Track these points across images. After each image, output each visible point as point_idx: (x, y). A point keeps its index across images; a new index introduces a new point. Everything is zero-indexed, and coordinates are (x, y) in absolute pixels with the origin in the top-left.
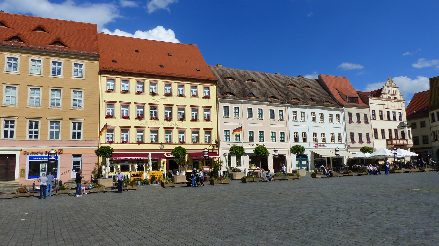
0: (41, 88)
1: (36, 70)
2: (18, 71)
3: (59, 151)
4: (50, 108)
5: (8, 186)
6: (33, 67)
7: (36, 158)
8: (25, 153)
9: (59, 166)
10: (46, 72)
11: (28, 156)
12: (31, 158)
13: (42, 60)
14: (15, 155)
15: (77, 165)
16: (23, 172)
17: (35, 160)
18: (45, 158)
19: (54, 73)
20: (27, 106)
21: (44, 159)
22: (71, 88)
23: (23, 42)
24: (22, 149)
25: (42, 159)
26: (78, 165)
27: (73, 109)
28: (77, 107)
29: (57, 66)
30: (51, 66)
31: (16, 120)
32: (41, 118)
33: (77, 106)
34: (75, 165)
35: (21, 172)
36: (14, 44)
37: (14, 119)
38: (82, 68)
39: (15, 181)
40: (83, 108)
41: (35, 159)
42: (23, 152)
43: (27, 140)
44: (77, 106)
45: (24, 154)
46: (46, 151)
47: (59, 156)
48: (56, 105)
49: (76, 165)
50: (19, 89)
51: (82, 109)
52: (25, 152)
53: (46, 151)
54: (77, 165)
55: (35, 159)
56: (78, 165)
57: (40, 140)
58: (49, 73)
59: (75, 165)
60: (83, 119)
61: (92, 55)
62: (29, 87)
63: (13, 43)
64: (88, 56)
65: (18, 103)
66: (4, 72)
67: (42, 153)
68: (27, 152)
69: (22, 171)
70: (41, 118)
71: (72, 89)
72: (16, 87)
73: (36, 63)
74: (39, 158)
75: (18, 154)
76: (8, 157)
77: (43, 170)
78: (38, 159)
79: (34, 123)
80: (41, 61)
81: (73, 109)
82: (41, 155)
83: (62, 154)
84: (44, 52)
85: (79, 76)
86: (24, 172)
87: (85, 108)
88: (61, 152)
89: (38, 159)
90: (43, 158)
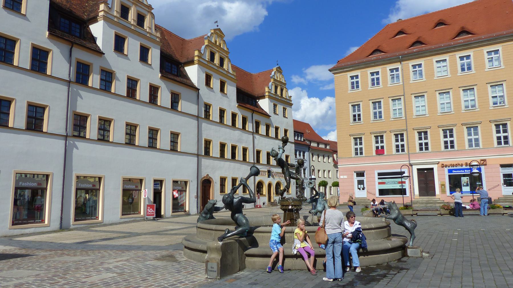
0: (451, 91)
1: (442, 71)
2: (424, 77)
3: (482, 162)
4: (464, 111)
5: (430, 202)
6: (439, 69)
7: (455, 172)
8: (443, 166)
9: (485, 180)
10: (454, 71)
11: (446, 170)
12: (450, 171)
13: (447, 58)
14: (432, 169)
15: (508, 179)
16: (443, 187)
17: (455, 173)
18: (466, 171)
19: (463, 69)
20: (438, 114)
21: (465, 172)
22: (487, 83)
23: (424, 44)
24: (439, 162)
25: (463, 172)
26: (509, 178)
27: (493, 108)
28: (499, 105)
29: (465, 61)
30: (459, 62)
31: (428, 131)
32: (455, 125)
33: (498, 103)
34: (505, 179)
35: (442, 187)
36: (416, 50)
37: (427, 130)
38: (498, 55)
39: (437, 197)
40: (507, 105)
41: (455, 173)
42: (440, 165)
43: (443, 152)
44: (498, 103)
45: (442, 167)
46: (466, 162)
47: (483, 168)
48: (471, 108)
49: (506, 178)
50: (427, 97)
51: (505, 107)
52: (443, 164)
53: (466, 163)
54: (508, 179)
55: (455, 173)
56: (509, 178)
57: (457, 150)
58: (457, 71)
59: (505, 179)
60: (510, 119)
61: (510, 35)
62: (437, 93)
63: (415, 49)
64: (504, 37)
65: (429, 112)
66: (411, 82)
67: (462, 165)
68: (445, 164)
69: (443, 186)
70: (455, 125)
71: (488, 84)
72: (424, 95)
73: (442, 64)
74: (459, 171)
75: (435, 167)
76: (426, 171)
77: (465, 184)
78: (458, 173)
79: (448, 132)
80: (446, 60)
81: (493, 108)
82: (461, 167)
83: (486, 165)
84: (448, 48)
85: (496, 66)
86: (445, 187)
87: (509, 104)
88: (485, 163)
89: (458, 173)
90: (463, 171)
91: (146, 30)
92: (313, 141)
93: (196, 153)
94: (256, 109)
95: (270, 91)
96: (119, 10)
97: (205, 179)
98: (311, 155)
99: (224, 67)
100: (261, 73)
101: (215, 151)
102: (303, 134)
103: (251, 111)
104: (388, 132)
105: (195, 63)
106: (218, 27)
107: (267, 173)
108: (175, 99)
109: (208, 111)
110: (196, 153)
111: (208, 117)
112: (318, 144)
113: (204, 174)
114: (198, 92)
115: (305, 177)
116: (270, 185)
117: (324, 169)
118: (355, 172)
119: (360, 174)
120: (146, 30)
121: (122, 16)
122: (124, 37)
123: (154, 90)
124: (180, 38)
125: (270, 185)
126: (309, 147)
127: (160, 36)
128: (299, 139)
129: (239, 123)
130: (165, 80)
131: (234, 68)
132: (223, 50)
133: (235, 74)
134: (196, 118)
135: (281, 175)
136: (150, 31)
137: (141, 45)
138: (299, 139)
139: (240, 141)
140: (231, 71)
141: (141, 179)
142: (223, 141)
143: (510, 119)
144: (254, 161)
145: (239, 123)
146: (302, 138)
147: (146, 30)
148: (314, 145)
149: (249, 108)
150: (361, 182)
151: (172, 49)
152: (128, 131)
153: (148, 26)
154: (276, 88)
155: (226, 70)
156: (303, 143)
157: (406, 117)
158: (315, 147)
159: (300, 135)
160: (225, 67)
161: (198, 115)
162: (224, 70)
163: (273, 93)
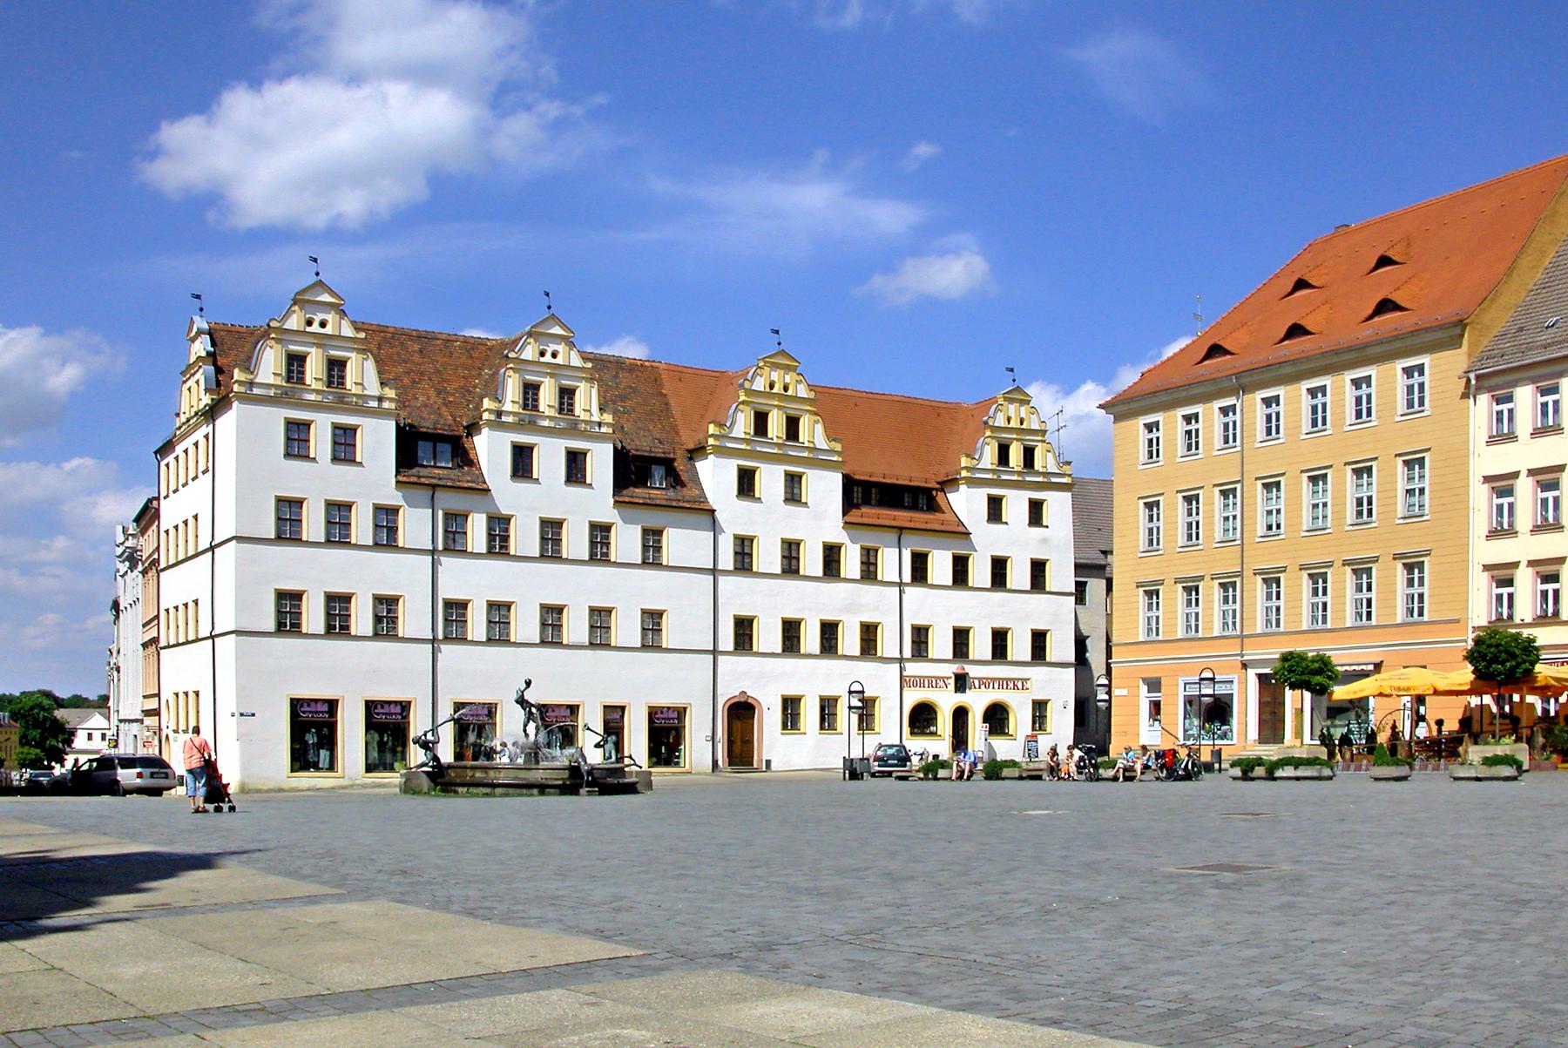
51: (1425, 518)
60: (1427, 553)
93: (712, 648)
96: (519, 397)
97: (738, 702)
101: (768, 636)
103: (896, 530)
104: (1207, 578)
106: (781, 347)
108: (652, 540)
109: (747, 554)
111: (746, 566)
113: (728, 692)
118: (1144, 680)
119: (1154, 685)
123: (600, 534)
124: (713, 371)
127: (611, 421)
129: (851, 563)
139: (850, 608)
140: (821, 442)
143: (1427, 553)
145: (851, 563)
150: (1156, 708)
152: (739, 550)
157: (1242, 540)
160: (804, 435)
163: (990, 467)
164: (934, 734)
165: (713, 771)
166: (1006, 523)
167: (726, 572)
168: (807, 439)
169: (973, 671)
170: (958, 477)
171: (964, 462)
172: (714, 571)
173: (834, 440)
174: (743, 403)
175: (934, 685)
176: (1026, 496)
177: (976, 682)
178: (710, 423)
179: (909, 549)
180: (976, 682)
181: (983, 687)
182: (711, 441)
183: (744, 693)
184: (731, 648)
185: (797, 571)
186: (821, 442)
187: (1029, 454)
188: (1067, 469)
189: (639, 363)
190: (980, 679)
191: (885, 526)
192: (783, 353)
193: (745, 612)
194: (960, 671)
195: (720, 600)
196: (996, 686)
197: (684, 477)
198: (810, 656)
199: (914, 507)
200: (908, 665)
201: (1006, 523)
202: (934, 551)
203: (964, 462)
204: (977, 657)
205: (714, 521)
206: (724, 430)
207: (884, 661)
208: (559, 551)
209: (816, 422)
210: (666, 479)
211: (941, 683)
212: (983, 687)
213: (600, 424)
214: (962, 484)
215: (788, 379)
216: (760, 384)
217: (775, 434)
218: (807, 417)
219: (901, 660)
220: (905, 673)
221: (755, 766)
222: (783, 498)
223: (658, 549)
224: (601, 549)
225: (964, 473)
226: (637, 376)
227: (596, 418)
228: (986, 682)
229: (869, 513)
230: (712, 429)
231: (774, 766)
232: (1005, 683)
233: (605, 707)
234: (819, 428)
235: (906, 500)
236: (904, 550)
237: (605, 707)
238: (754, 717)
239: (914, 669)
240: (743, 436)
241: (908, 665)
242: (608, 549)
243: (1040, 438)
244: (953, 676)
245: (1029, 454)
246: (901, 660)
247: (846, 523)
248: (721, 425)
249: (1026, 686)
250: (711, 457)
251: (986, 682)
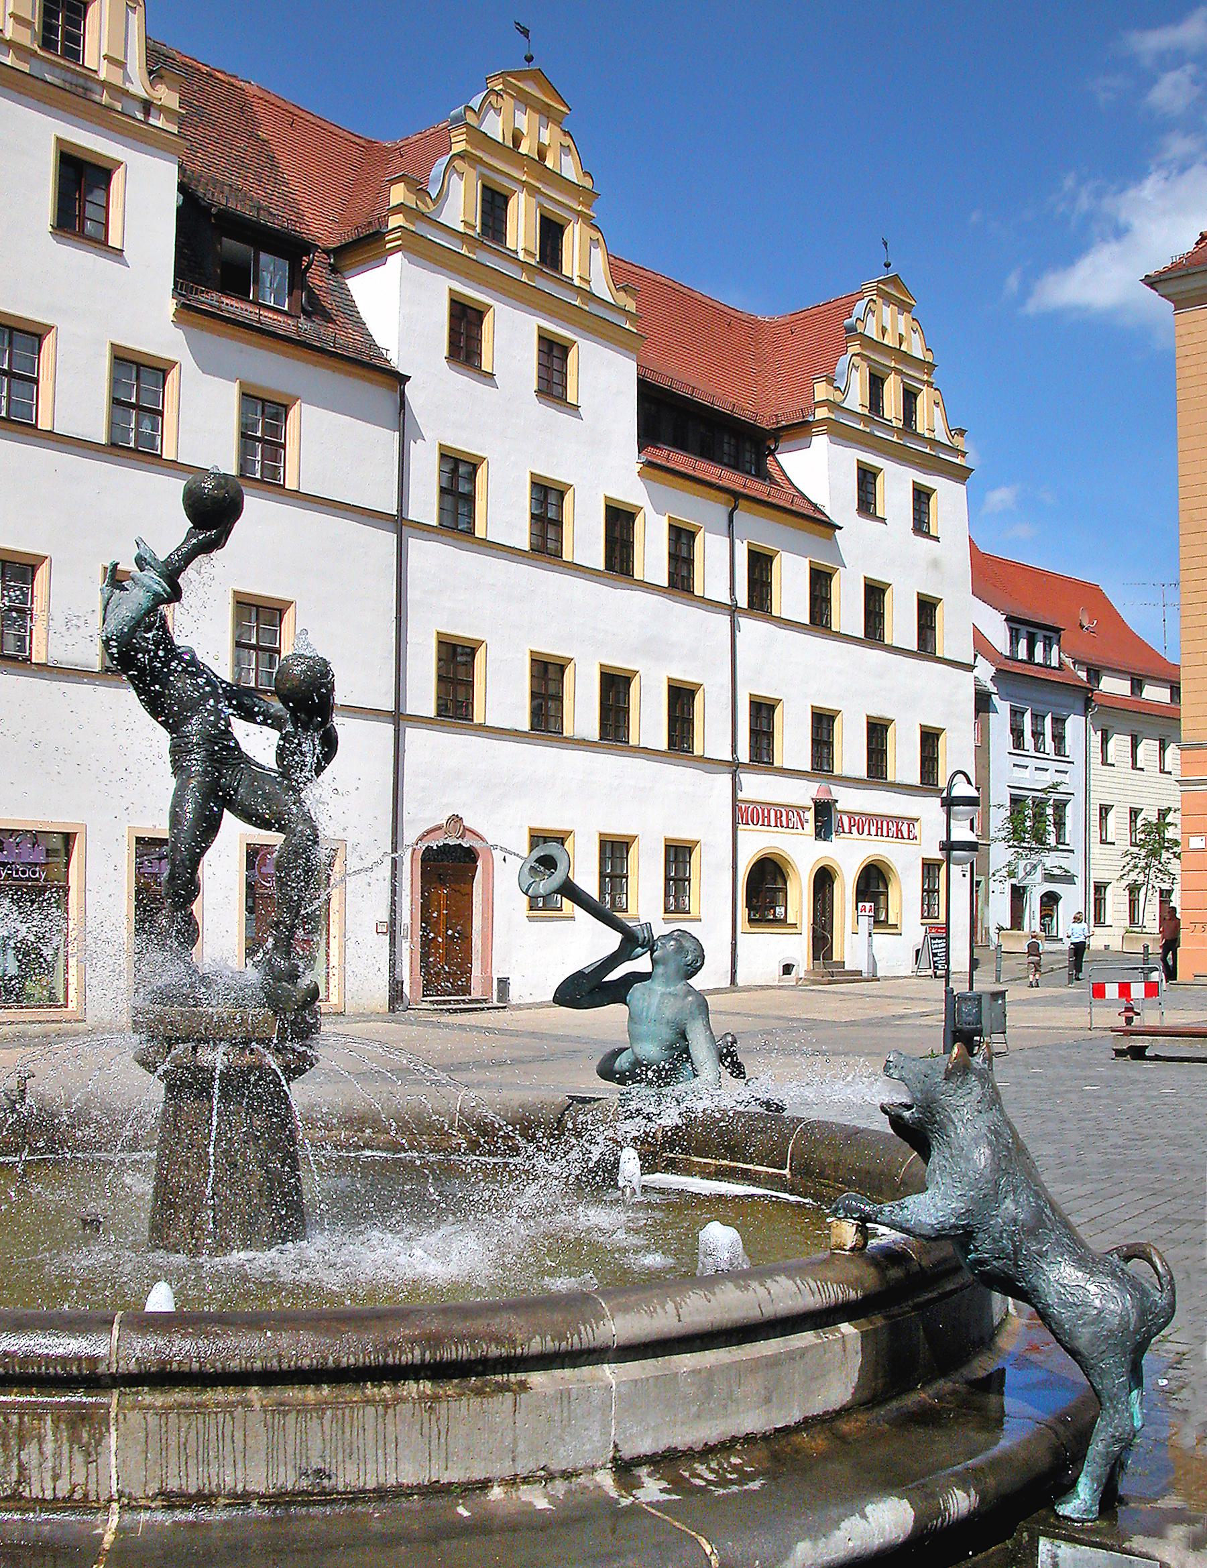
91: (93, 75)
92: (1109, 669)
93: (390, 706)
94: (757, 488)
95: (838, 397)
98: (1096, 738)
99: (510, 244)
100: (802, 315)
102: (1057, 630)
105: (388, 246)
106: (533, 66)
107: (810, 815)
110: (390, 706)
112: (1137, 685)
114: (403, 394)
115: (1063, 844)
116: (824, 879)
117: (1137, 800)
120: (93, 75)
121: (48, 43)
122: (105, 165)
125: (824, 879)
126: (1086, 699)
128: (1039, 657)
130: (194, 325)
131: (620, 272)
132: (556, 178)
133: (631, 306)
134: (390, 525)
135: (894, 829)
136: (116, 78)
137: (65, 150)
138: (1022, 654)
140: (602, 287)
141: (68, 834)
142: (551, 648)
144: (734, 751)
146: (1055, 648)
147: (95, 72)
148: (1114, 686)
149: (691, 472)
151: (286, 184)
153: (10, 10)
154: (876, 383)
155: (577, 282)
156: (1056, 677)
158: (1121, 698)
159: (1045, 637)
160: (571, 265)
161: (400, 510)
162: (567, 283)
163: (859, 410)
164: (783, 922)
165: (392, 1010)
166: (883, 520)
167: (423, 529)
168: (577, 273)
169: (848, 800)
170: (811, 419)
171: (822, 391)
172: (399, 523)
173: (624, 289)
174: (461, 156)
175: (784, 824)
176: (912, 475)
177: (845, 819)
178: (394, 181)
179: (745, 542)
180: (845, 819)
181: (854, 829)
182: (395, 221)
183: (456, 819)
184: (430, 710)
185: (558, 554)
186: (602, 287)
187: (910, 397)
188: (958, 442)
189: (204, 69)
190: (850, 814)
191: (710, 485)
192: (538, 76)
193: (462, 630)
194: (824, 797)
195: (412, 595)
196: (873, 831)
197: (328, 302)
198: (582, 744)
199: (736, 465)
200: (745, 778)
201: (883, 520)
202: (783, 553)
203: (822, 391)
204: (847, 772)
205: (403, 403)
206: (425, 204)
207: (708, 766)
208: (31, 407)
209: (594, 243)
210: (290, 294)
211: (795, 819)
212: (854, 829)
213: (147, 106)
214: (819, 434)
215: (546, 136)
216: (494, 126)
217: (522, 245)
218: (577, 227)
219: (734, 767)
220: (741, 796)
221: (475, 995)
222: (535, 388)
223: (275, 448)
224: (138, 424)
225: (822, 413)
226: (201, 90)
227: (138, 86)
228: (863, 821)
229: (681, 461)
230: (398, 194)
231: (514, 995)
232: (885, 823)
233: (139, 840)
234: (599, 258)
235: (726, 446)
236: (737, 542)
237: (139, 840)
238: (473, 877)
239: (756, 786)
240: (461, 228)
241: (745, 778)
242: (155, 429)
243: (925, 378)
244: (812, 805)
245: (910, 397)
246: (734, 767)
247: (650, 464)
248: (421, 192)
249: (916, 832)
250: (396, 260)
251: (863, 821)
